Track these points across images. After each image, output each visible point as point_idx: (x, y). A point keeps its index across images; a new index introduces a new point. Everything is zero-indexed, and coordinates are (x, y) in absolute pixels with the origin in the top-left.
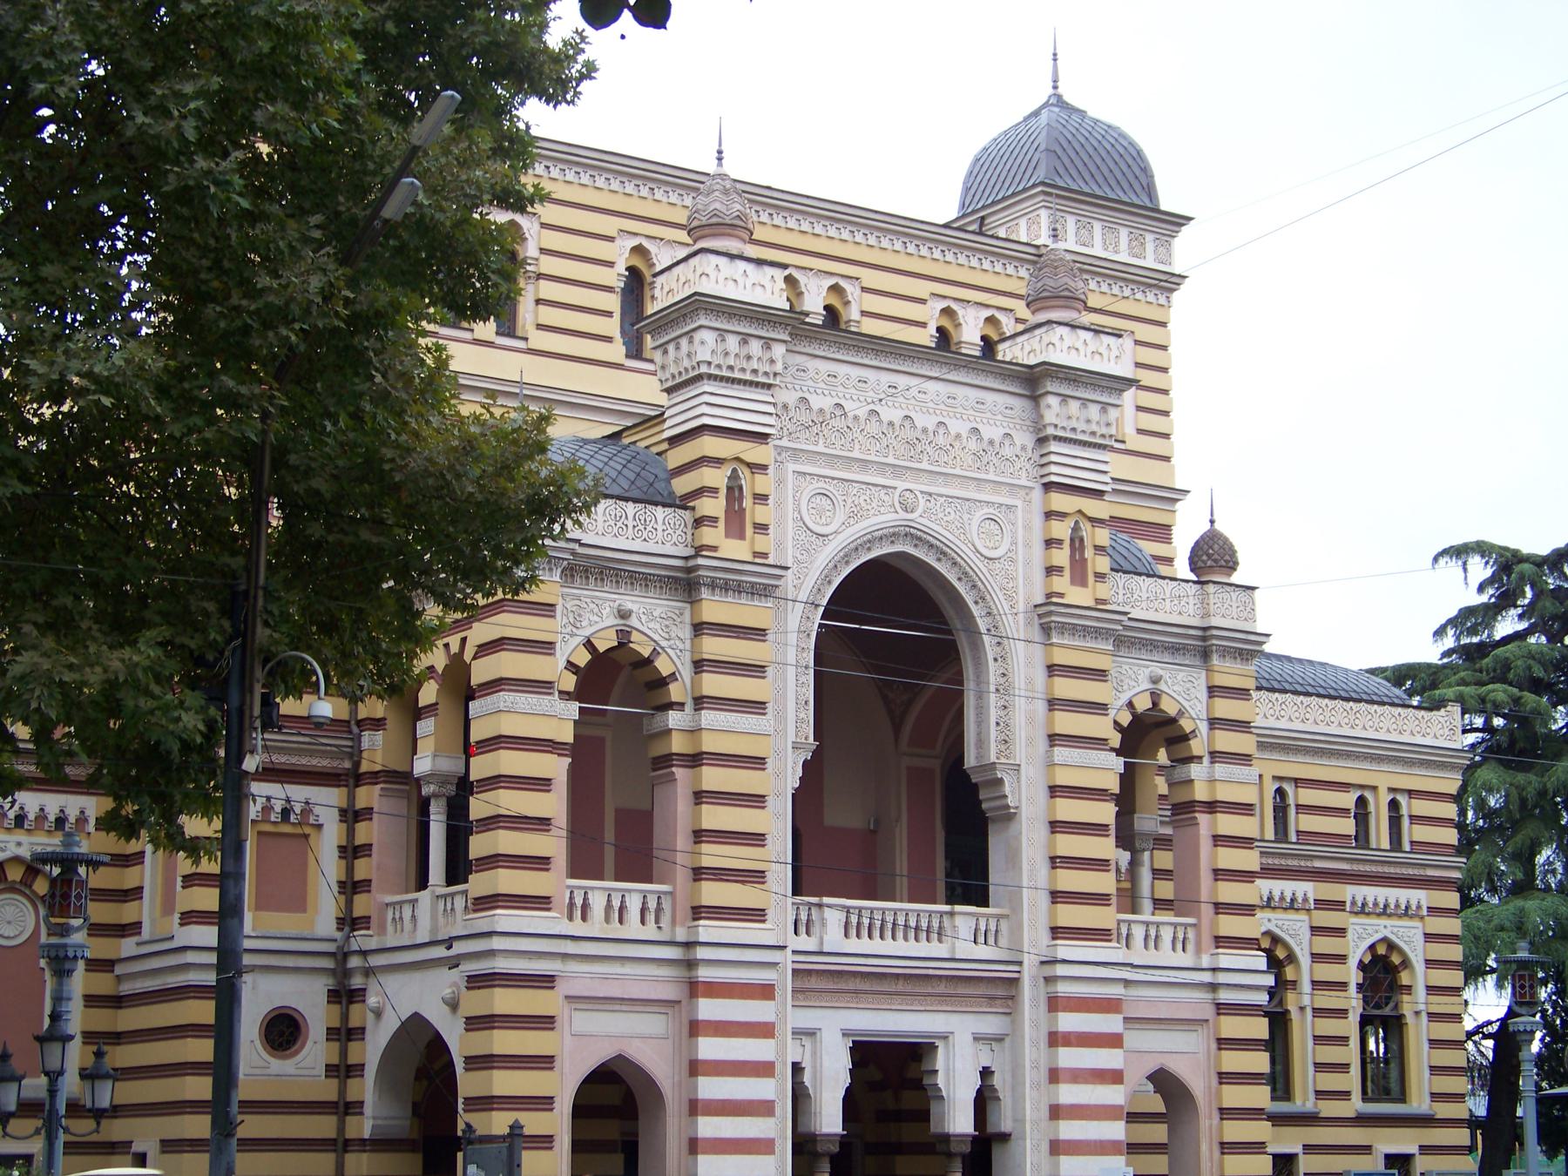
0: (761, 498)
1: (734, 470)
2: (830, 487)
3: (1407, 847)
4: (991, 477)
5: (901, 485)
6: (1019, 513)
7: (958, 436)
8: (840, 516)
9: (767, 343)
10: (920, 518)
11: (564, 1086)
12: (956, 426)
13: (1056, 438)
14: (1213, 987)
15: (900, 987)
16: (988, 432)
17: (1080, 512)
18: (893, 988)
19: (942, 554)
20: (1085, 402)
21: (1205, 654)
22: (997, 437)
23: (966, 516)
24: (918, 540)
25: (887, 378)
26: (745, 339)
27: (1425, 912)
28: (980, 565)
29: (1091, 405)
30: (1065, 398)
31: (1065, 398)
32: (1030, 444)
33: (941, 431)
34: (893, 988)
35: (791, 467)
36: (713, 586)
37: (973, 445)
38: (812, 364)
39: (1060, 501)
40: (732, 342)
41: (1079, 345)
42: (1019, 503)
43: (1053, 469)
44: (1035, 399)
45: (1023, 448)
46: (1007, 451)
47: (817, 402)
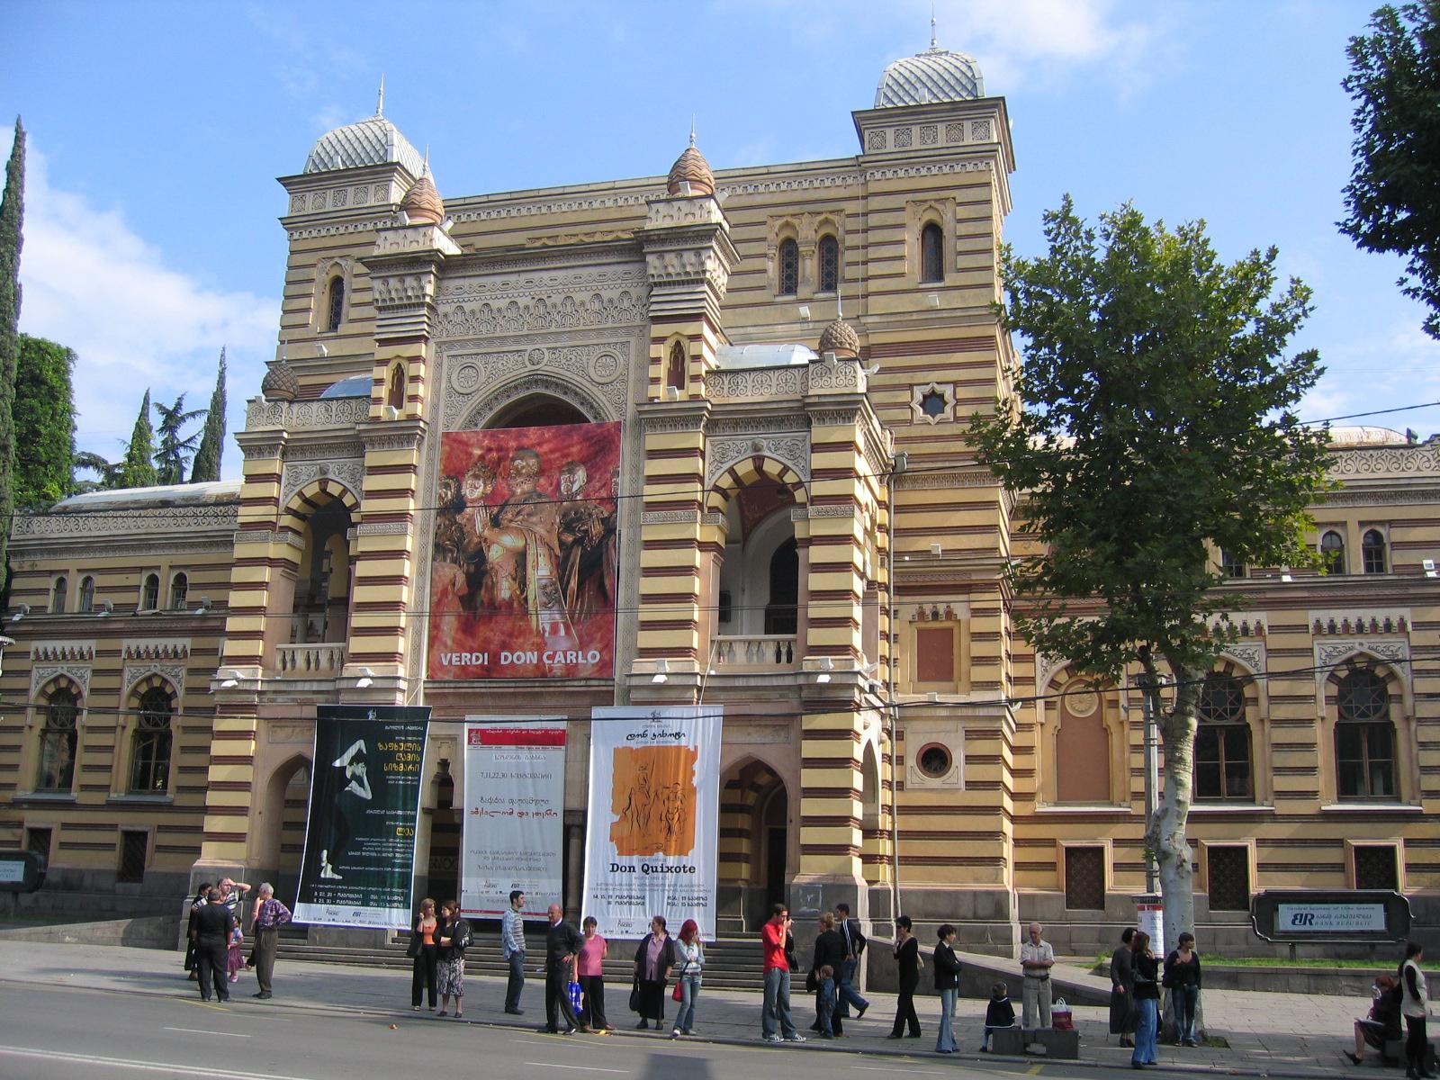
0: (415, 379)
1: (399, 365)
2: (479, 362)
3: (1390, 571)
4: (610, 325)
5: (530, 348)
6: (633, 345)
7: (583, 304)
8: (483, 378)
9: (418, 276)
10: (547, 366)
11: (258, 775)
12: (578, 297)
13: (656, 284)
14: (800, 687)
15: (519, 702)
16: (606, 295)
17: (677, 333)
18: (513, 703)
19: (566, 390)
20: (679, 253)
21: (809, 423)
22: (615, 294)
23: (584, 359)
24: (547, 384)
25: (524, 277)
26: (401, 278)
27: (1409, 627)
28: (596, 391)
29: (686, 255)
30: (661, 254)
31: (661, 254)
32: (643, 291)
33: (569, 303)
34: (513, 703)
35: (445, 354)
36: (372, 442)
37: (597, 306)
38: (466, 282)
39: (658, 330)
40: (393, 283)
41: (674, 212)
42: (633, 340)
43: (653, 307)
44: (644, 261)
45: (639, 299)
46: (626, 304)
47: (468, 307)
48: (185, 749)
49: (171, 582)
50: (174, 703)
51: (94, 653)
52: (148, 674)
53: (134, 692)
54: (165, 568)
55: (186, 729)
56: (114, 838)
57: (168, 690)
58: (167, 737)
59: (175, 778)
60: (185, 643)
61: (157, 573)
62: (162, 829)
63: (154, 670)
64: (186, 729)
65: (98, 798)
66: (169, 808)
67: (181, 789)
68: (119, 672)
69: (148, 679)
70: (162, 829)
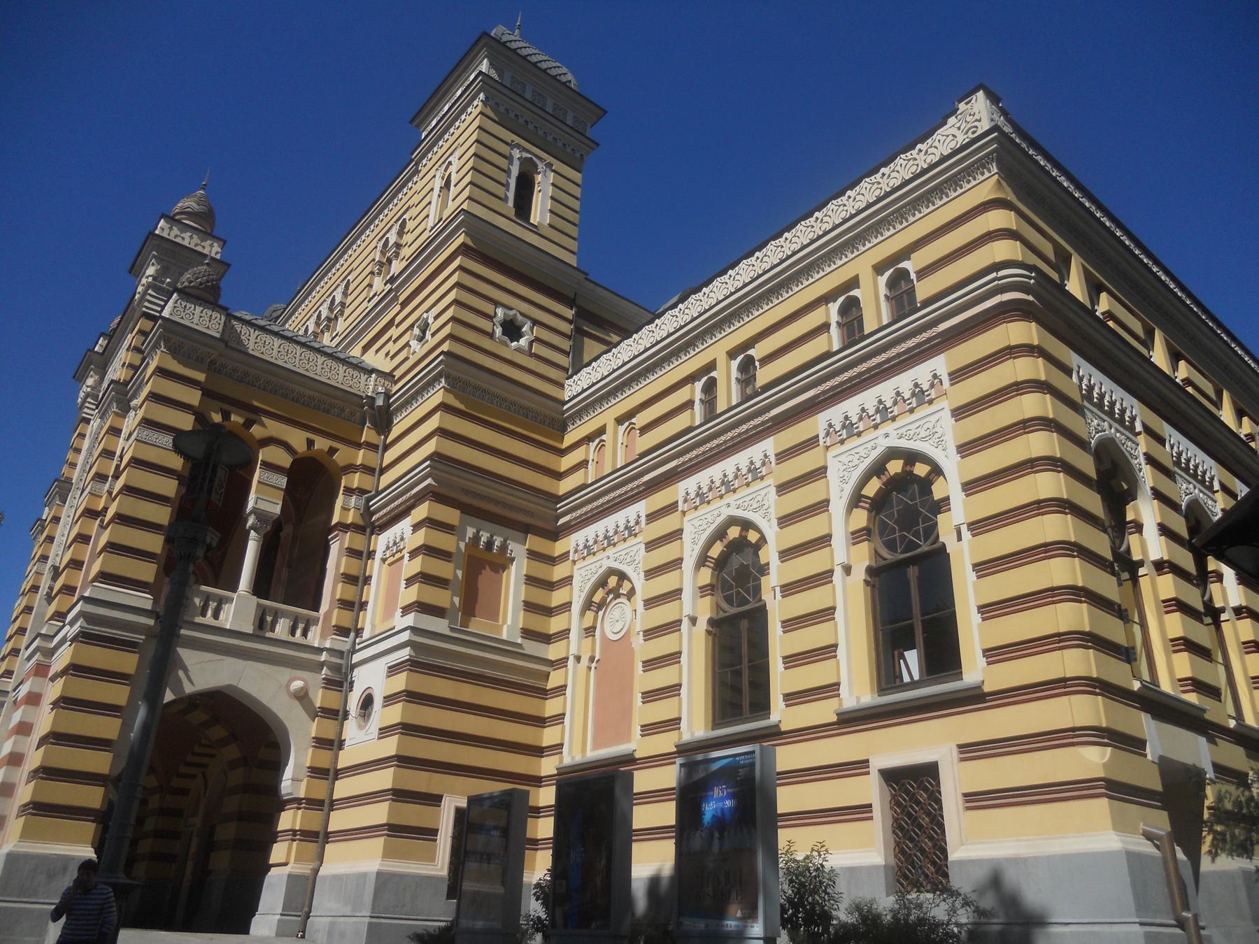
48: (984, 568)
49: (883, 290)
50: (938, 491)
51: (773, 459)
52: (874, 455)
53: (856, 500)
54: (866, 276)
55: (979, 526)
56: (869, 790)
57: (921, 470)
58: (939, 558)
59: (973, 634)
60: (940, 364)
61: (854, 293)
62: (970, 751)
63: (883, 444)
64: (979, 526)
65: (824, 712)
66: (975, 698)
67: (995, 654)
68: (820, 472)
69: (878, 469)
70: (970, 751)
